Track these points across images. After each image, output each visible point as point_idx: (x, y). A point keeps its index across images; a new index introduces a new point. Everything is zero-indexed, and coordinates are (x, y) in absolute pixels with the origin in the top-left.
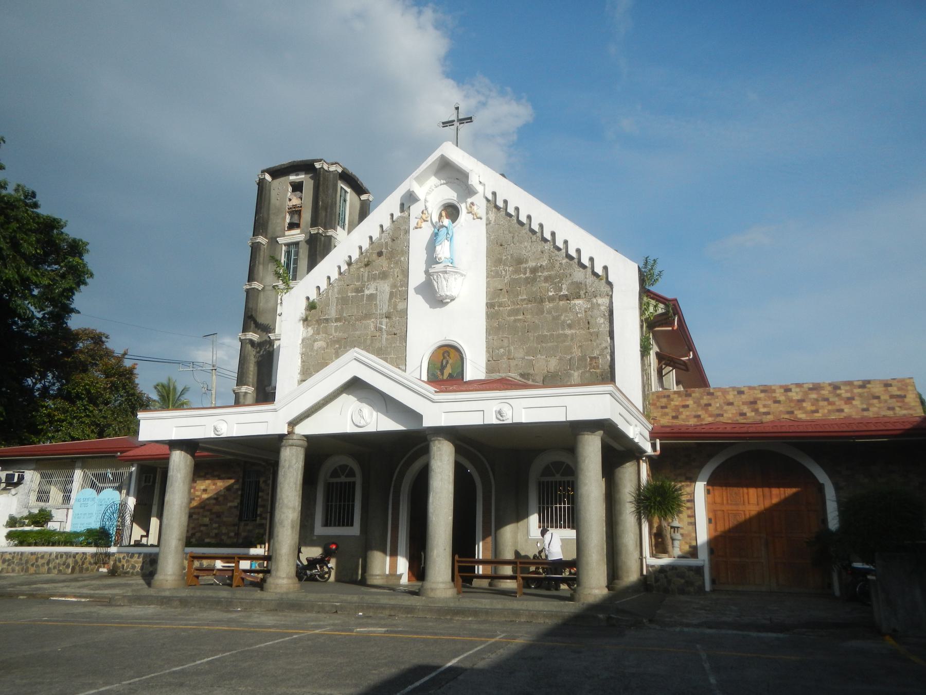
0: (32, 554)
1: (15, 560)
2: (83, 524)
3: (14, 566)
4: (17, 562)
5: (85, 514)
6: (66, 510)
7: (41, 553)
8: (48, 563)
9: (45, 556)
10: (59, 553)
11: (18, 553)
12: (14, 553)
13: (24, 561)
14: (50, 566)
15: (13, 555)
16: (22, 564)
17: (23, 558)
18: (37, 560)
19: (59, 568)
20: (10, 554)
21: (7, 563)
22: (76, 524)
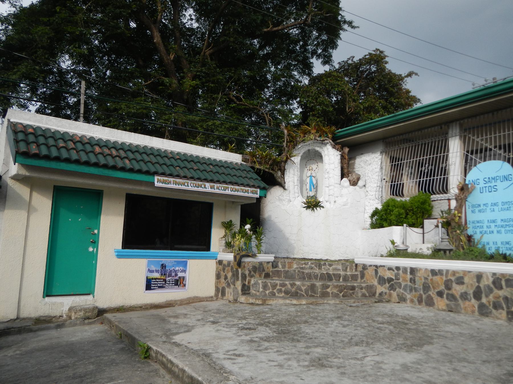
0: (434, 272)
1: (400, 281)
2: (494, 221)
3: (401, 291)
4: (406, 286)
5: (495, 204)
6: (447, 201)
7: (454, 273)
8: (477, 294)
9: (466, 280)
10: (503, 275)
11: (405, 269)
12: (398, 268)
13: (419, 284)
14: (484, 300)
15: (396, 271)
16: (416, 290)
17: (417, 279)
18: (448, 286)
19: (508, 308)
20: (390, 269)
21: (387, 285)
22: (478, 222)
